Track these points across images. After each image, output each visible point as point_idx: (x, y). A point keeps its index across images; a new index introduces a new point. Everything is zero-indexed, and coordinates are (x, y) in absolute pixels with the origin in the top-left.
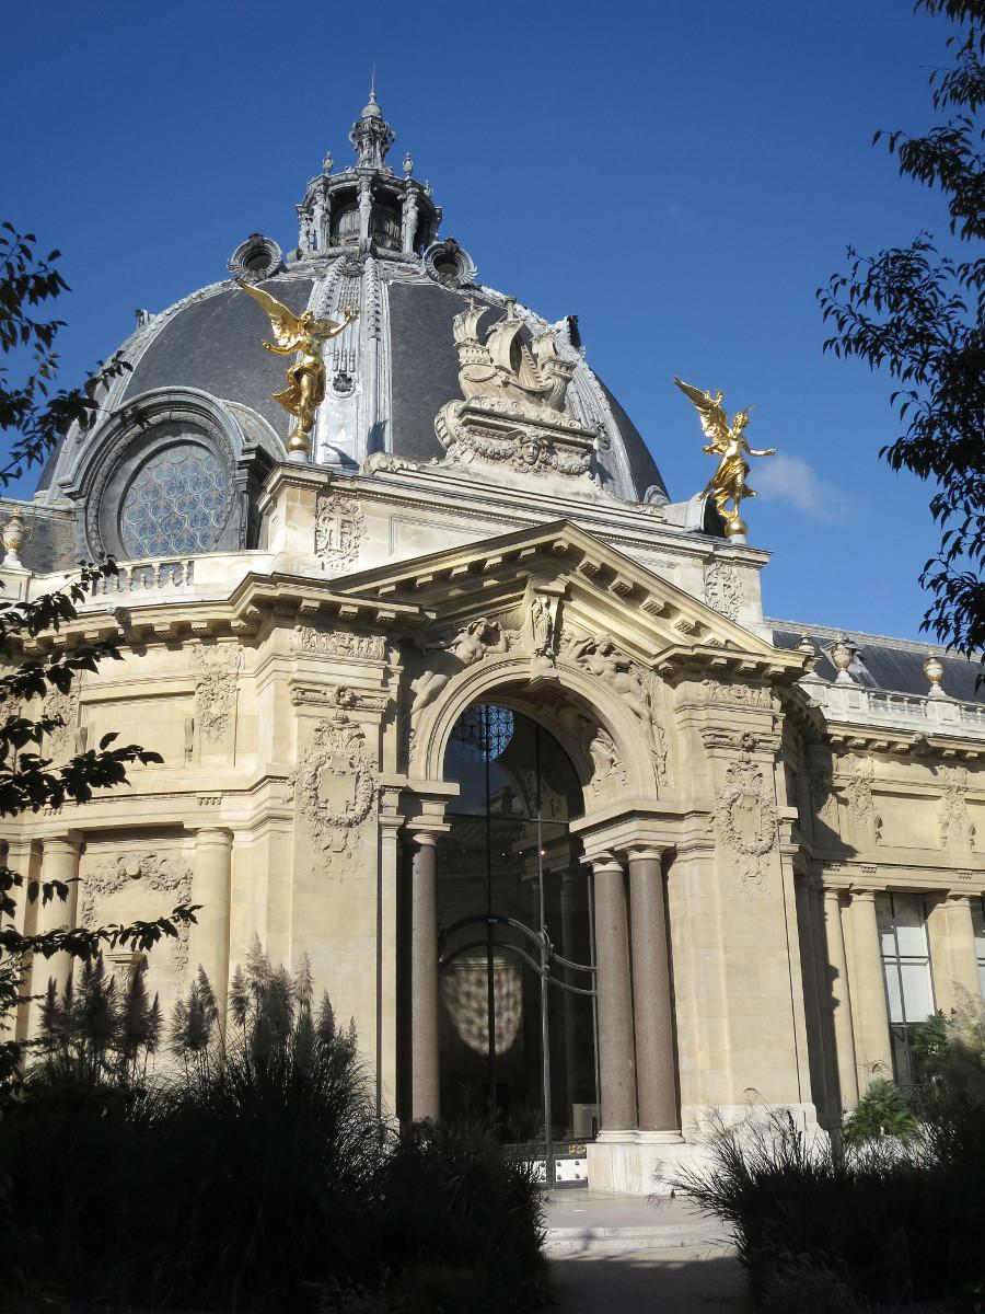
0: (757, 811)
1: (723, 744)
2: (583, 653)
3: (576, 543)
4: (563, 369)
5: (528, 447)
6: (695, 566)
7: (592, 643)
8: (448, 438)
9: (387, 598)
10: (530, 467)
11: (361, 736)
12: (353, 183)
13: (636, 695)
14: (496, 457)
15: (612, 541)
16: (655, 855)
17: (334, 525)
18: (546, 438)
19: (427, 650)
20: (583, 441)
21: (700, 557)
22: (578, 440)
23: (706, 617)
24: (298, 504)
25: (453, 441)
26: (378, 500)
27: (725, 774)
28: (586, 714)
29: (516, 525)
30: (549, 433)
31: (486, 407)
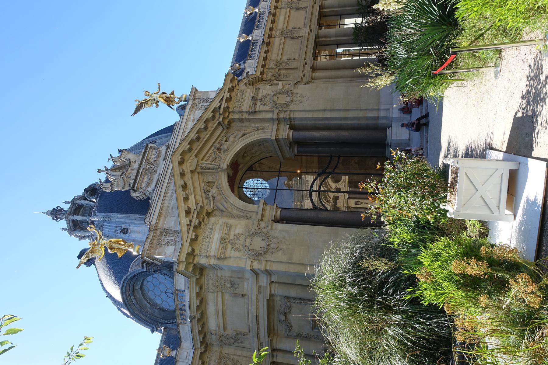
0: (279, 95)
8: (143, 196)
9: (191, 221)
10: (156, 168)
12: (71, 222)
14: (150, 180)
16: (291, 132)
22: (148, 150)
23: (210, 109)
24: (157, 251)
25: (145, 194)
26: (159, 221)
28: (242, 153)
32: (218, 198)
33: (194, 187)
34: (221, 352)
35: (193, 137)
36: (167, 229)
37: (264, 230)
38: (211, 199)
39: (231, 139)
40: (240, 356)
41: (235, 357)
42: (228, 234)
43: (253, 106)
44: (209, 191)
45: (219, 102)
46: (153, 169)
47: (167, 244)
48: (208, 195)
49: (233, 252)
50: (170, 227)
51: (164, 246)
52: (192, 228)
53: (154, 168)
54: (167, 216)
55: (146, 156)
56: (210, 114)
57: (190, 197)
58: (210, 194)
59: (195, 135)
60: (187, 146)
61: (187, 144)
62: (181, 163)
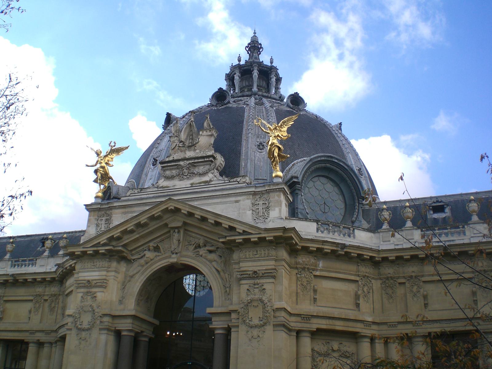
0: (261, 307)
1: (245, 278)
2: (196, 248)
3: (176, 206)
4: (208, 131)
5: (184, 169)
6: (247, 199)
7: (197, 244)
10: (186, 177)
11: (95, 297)
13: (217, 262)
14: (171, 178)
15: (185, 201)
17: (103, 222)
18: (190, 163)
19: (134, 260)
20: (208, 159)
21: (250, 194)
22: (206, 160)
27: (246, 291)
29: (148, 205)
30: (193, 161)
31: (171, 159)
32: (142, 261)
33: (151, 233)
34: (59, 295)
35: (196, 214)
36: (112, 219)
37: (98, 322)
38: (142, 255)
39: (212, 256)
40: (57, 313)
41: (56, 309)
42: (96, 286)
43: (247, 276)
44: (149, 250)
45: (244, 231)
46: (184, 174)
47: (97, 225)
48: (146, 250)
49: (81, 295)
50: (114, 222)
51: (96, 222)
52: (95, 249)
53: (185, 176)
54: (125, 214)
55: (199, 161)
56: (226, 224)
57: (135, 233)
58: (146, 252)
59: (198, 215)
60: (186, 211)
61: (187, 210)
62: (166, 211)
